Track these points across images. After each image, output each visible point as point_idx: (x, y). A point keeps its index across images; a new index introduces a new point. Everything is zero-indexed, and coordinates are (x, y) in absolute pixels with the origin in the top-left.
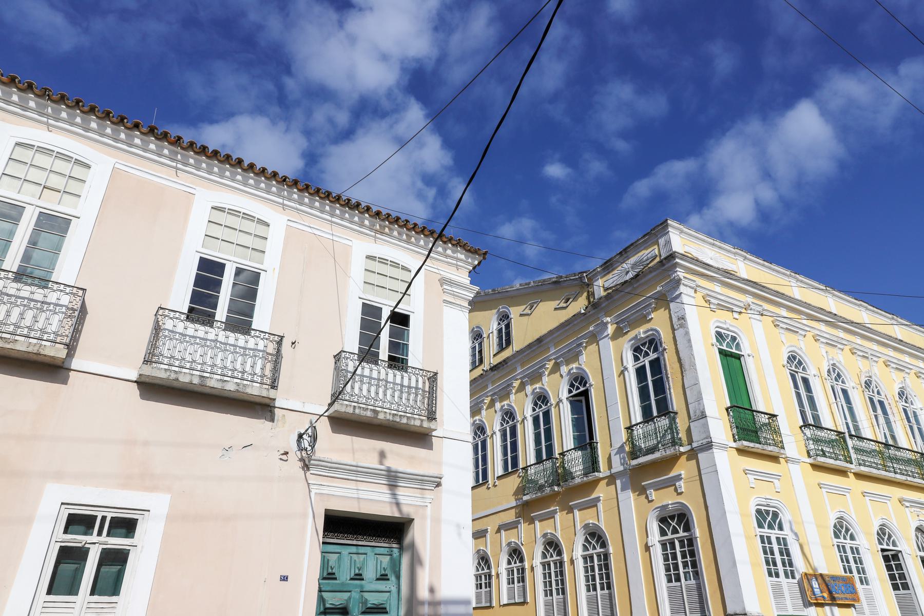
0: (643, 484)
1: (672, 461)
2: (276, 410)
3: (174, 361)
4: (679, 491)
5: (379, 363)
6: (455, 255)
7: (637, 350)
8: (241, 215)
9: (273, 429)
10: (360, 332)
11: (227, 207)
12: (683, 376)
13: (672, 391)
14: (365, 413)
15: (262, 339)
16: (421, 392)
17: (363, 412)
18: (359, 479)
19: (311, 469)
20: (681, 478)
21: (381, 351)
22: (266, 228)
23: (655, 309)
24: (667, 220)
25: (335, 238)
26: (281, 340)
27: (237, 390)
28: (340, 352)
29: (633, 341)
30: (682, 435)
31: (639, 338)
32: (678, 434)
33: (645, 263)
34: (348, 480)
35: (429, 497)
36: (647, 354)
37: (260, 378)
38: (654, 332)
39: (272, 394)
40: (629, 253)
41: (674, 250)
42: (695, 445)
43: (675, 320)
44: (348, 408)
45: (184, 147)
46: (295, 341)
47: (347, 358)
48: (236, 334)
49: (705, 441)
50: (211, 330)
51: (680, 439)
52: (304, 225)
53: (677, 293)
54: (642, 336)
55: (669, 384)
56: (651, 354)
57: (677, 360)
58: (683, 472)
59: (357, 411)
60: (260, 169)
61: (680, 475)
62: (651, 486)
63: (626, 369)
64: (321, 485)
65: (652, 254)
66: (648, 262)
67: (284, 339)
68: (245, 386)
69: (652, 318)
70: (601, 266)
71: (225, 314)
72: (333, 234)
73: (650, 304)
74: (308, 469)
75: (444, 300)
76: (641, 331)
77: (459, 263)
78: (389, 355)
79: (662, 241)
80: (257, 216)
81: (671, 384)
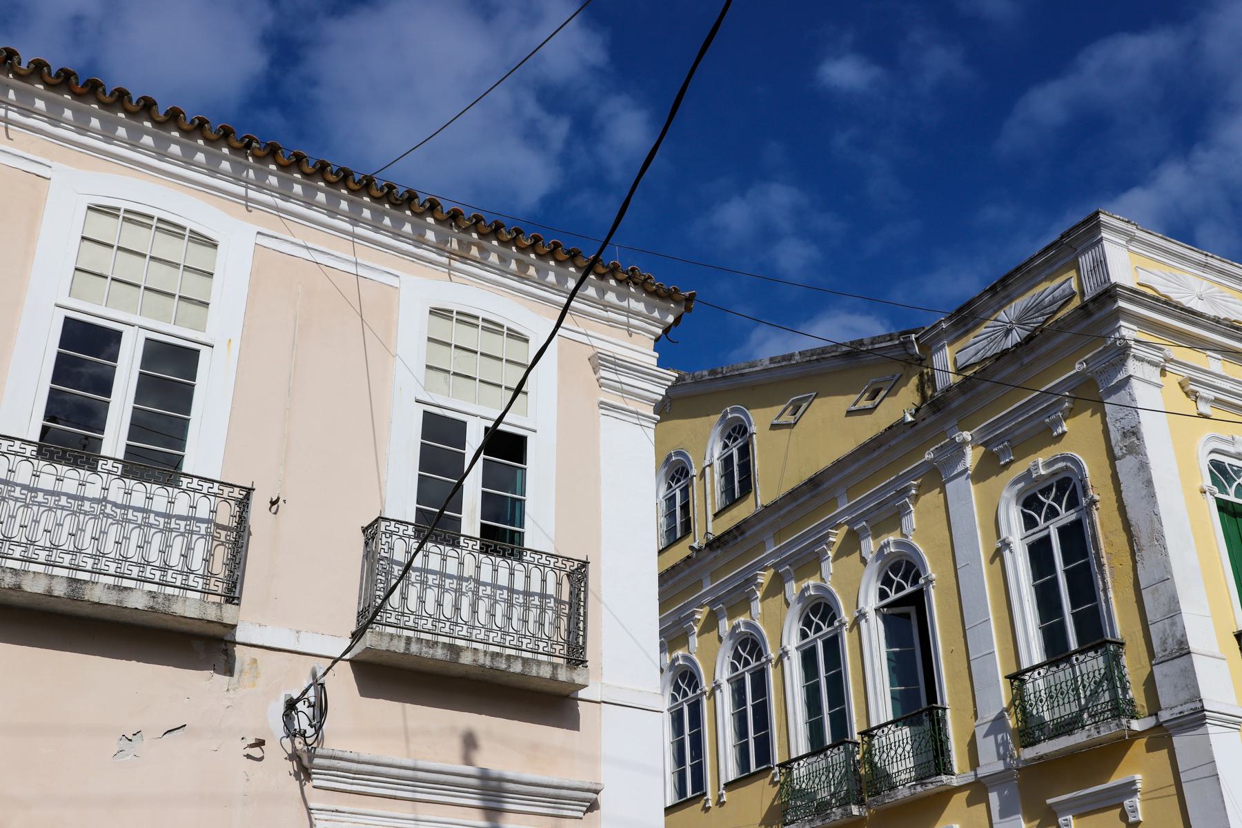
0: (1049, 801)
1: (1115, 750)
2: (238, 649)
3: (12, 547)
4: (1131, 819)
5: (462, 544)
6: (625, 304)
7: (1030, 503)
8: (154, 223)
9: (231, 691)
10: (419, 475)
11: (124, 205)
12: (1135, 562)
13: (1111, 594)
14: (431, 651)
15: (205, 495)
16: (552, 605)
17: (427, 650)
18: (419, 796)
19: (314, 776)
20: (1136, 791)
21: (464, 516)
22: (211, 250)
23: (1071, 413)
24: (1097, 213)
25: (361, 272)
26: (247, 497)
27: (152, 608)
28: (376, 521)
29: (1022, 484)
30: (1136, 693)
31: (1034, 476)
32: (1125, 690)
33: (1048, 310)
34: (395, 798)
36: (1053, 513)
37: (201, 581)
38: (1069, 464)
39: (229, 614)
40: (1011, 289)
41: (1113, 280)
42: (1164, 716)
43: (1115, 436)
44: (395, 642)
45: (22, 72)
46: (278, 499)
47: (392, 533)
48: (148, 485)
49: (1187, 708)
50: (92, 477)
51: (1131, 702)
52: (293, 243)
53: (1121, 376)
54: (1043, 472)
55: (1103, 579)
56: (1062, 511)
57: (1121, 526)
58: (1138, 777)
59: (414, 648)
60: (192, 122)
61: (1133, 783)
62: (1067, 807)
63: (1007, 545)
64: (337, 811)
65: (1064, 291)
66: (1055, 307)
67: (254, 495)
68: (168, 598)
69: (1064, 433)
70: (950, 318)
71: (123, 441)
72: (356, 263)
73: (1059, 403)
74: (308, 777)
75: (602, 403)
76: (1040, 462)
77: (633, 321)
78: (482, 524)
79: (1086, 261)
80: (190, 225)
81: (1108, 579)
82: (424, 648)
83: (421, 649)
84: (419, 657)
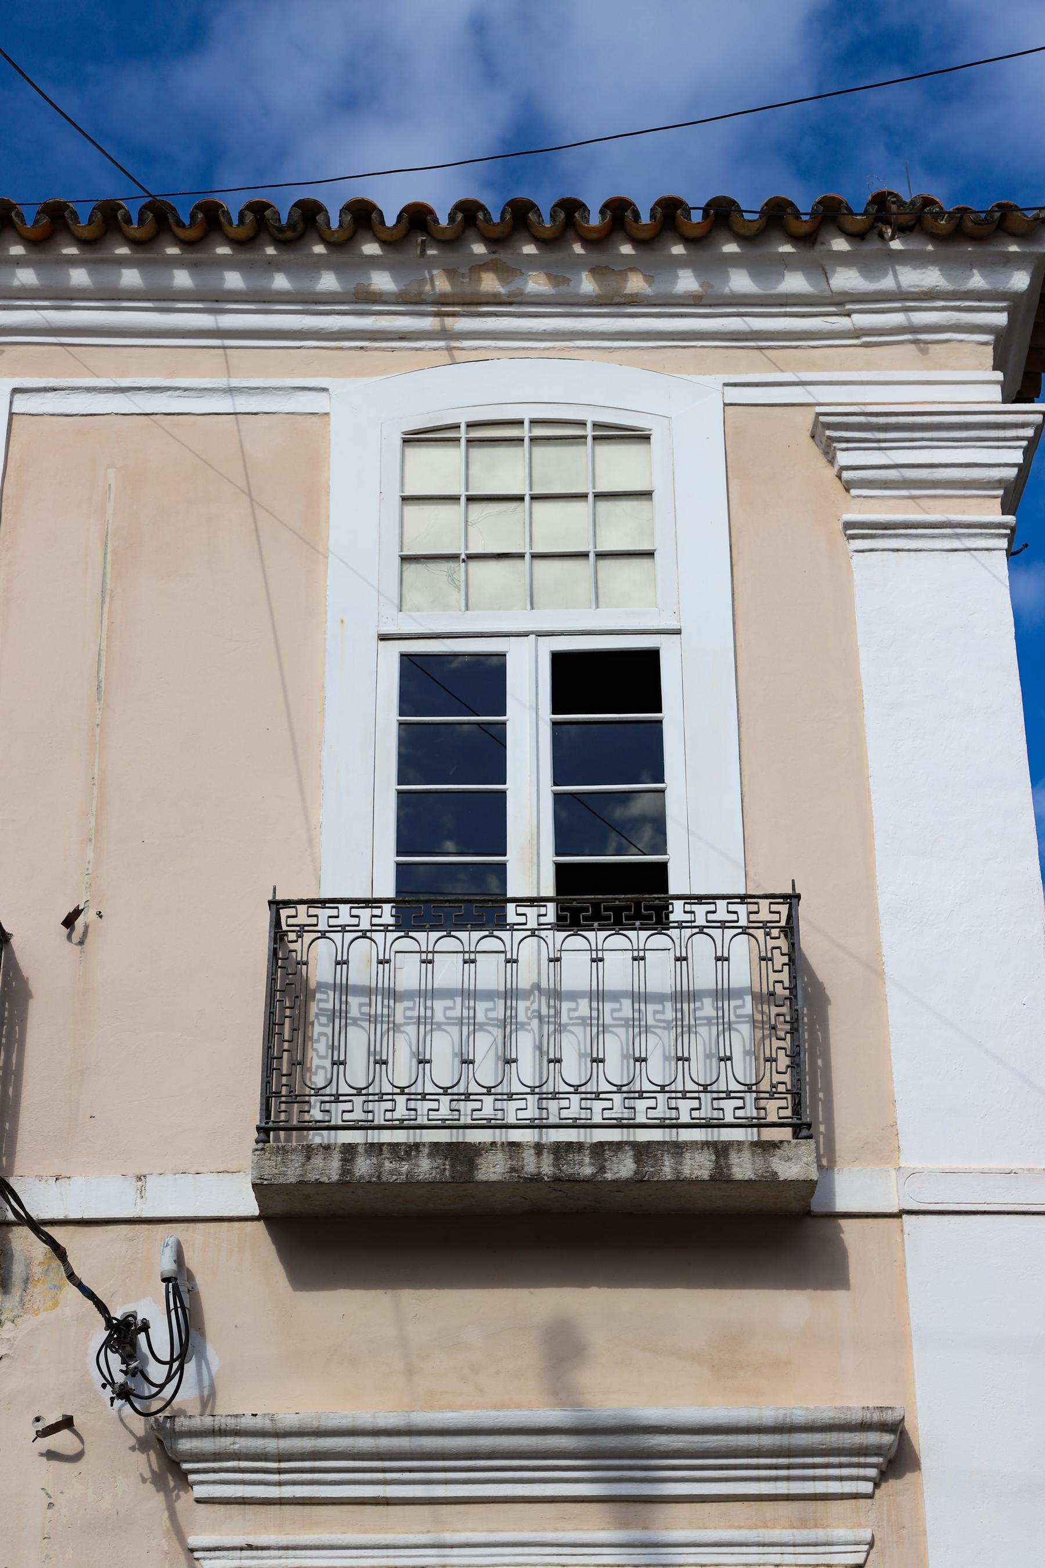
6: (887, 283)
14: (405, 1167)
16: (748, 1009)
19: (192, 1477)
34: (387, 1502)
35: (840, 1533)
44: (318, 1161)
59: (363, 1166)
74: (183, 1479)
75: (848, 525)
77: (921, 318)
82: (387, 1163)
83: (381, 1165)
84: (376, 1185)
